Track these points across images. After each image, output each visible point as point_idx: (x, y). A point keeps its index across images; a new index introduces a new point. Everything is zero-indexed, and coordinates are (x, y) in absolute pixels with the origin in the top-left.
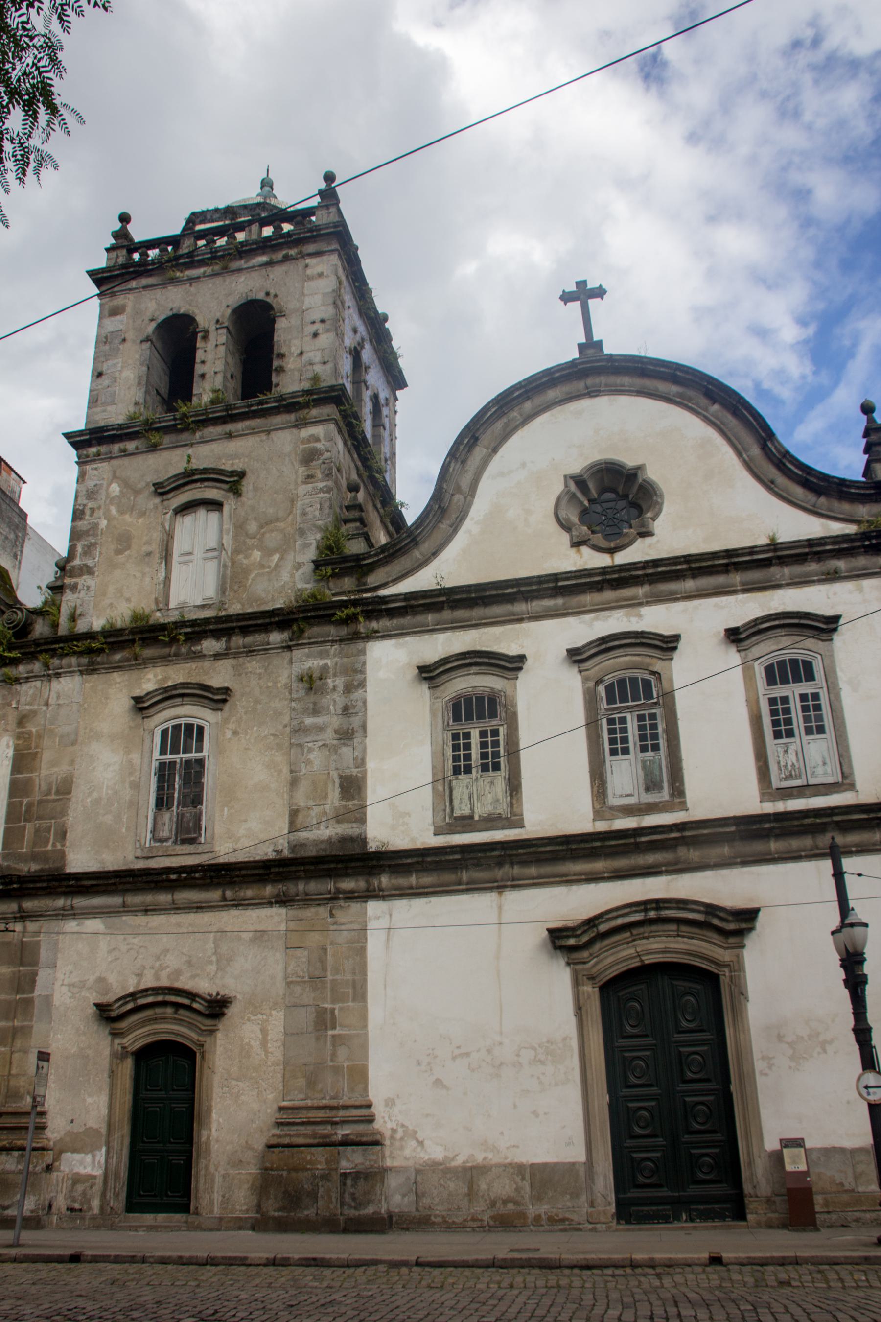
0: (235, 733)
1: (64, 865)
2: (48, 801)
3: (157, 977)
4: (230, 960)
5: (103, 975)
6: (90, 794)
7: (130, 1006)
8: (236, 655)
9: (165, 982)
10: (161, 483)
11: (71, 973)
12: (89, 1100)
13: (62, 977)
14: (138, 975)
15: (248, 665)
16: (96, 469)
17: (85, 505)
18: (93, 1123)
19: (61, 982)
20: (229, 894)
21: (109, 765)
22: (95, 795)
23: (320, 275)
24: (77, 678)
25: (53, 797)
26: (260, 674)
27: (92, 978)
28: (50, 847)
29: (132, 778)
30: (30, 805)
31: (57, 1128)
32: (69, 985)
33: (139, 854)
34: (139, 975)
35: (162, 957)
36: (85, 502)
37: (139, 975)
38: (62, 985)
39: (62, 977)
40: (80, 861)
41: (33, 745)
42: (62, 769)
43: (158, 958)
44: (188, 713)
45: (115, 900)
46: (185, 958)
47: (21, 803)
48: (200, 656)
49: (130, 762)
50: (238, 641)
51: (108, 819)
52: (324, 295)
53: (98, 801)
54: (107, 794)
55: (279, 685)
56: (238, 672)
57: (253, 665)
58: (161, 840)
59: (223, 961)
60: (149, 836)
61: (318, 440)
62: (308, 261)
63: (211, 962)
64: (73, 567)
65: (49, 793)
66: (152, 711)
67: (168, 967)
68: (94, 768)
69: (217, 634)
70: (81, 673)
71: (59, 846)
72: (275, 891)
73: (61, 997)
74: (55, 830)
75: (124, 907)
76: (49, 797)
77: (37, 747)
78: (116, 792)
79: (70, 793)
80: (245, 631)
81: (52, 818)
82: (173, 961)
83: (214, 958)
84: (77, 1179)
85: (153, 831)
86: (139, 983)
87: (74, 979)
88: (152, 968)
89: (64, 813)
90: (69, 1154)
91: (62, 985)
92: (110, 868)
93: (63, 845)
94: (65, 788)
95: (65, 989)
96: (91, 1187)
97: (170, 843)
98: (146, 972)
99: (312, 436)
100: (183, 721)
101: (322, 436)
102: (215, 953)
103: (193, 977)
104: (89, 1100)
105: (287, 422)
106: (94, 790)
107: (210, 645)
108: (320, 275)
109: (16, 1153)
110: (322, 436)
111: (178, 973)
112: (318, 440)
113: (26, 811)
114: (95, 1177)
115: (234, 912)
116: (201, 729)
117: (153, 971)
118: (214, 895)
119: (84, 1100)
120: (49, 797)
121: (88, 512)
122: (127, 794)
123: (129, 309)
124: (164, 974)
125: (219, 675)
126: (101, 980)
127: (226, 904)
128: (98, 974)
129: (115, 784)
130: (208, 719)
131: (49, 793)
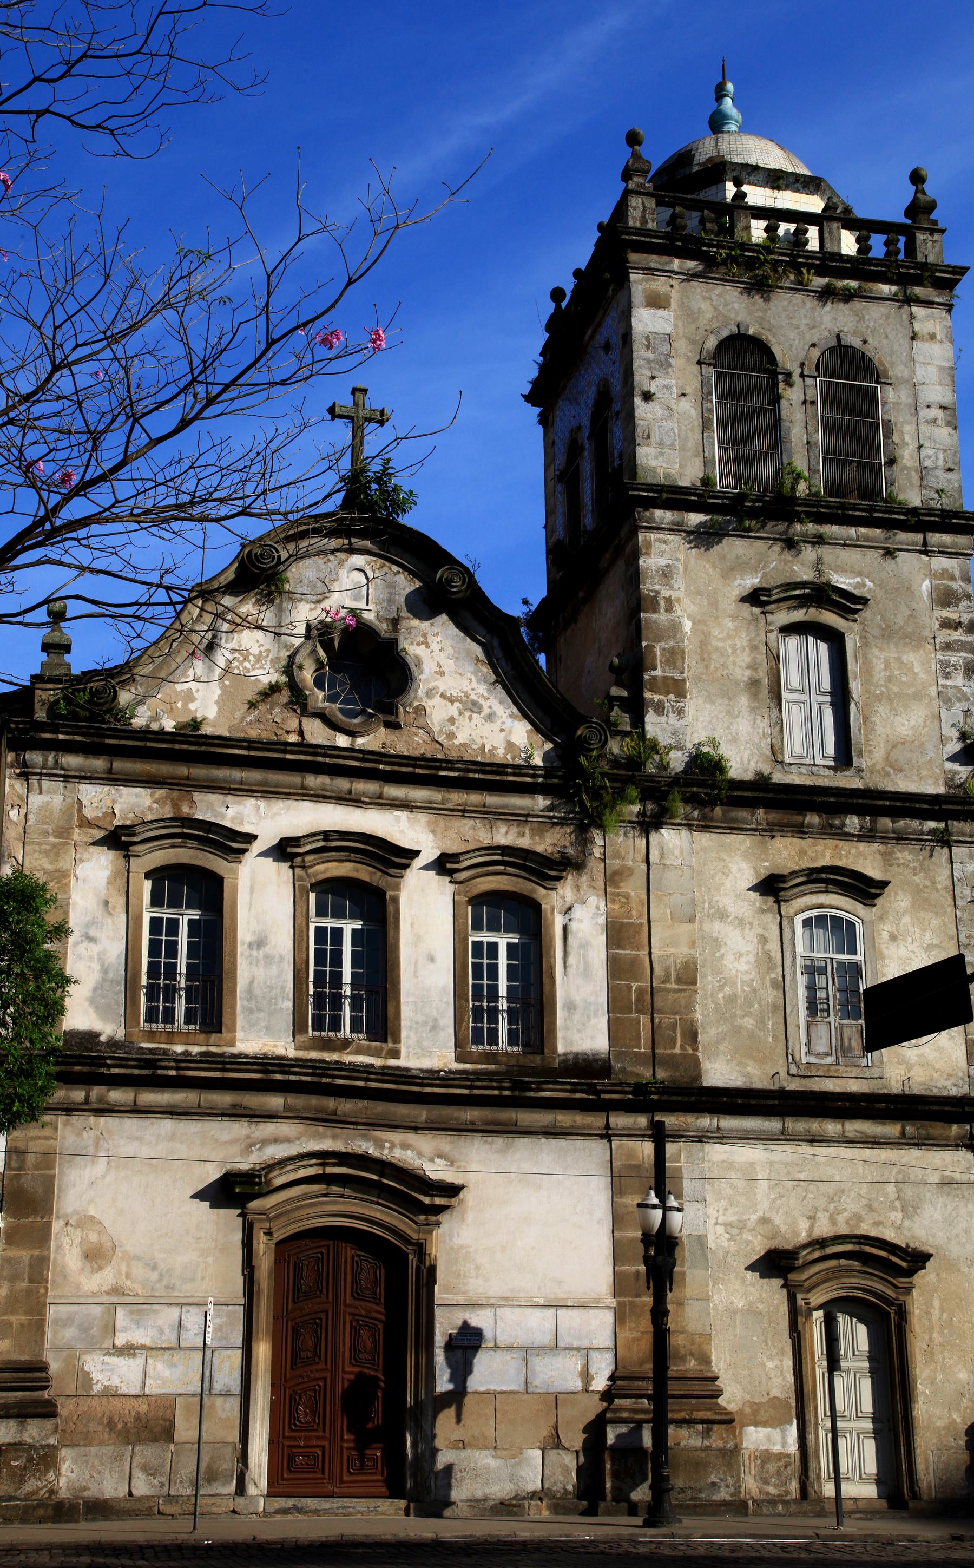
0: (893, 938)
1: (698, 1076)
2: (668, 991)
3: (834, 1222)
4: (915, 1208)
5: (767, 1215)
6: (721, 988)
7: (817, 1254)
8: (884, 839)
9: (844, 1230)
10: (769, 590)
11: (726, 1209)
12: (770, 1365)
13: (715, 1214)
14: (810, 1218)
15: (899, 855)
16: (665, 542)
17: (657, 592)
18: (775, 1392)
19: (714, 1221)
20: (909, 1130)
21: (741, 955)
22: (728, 990)
23: (933, 337)
24: (684, 833)
25: (674, 986)
26: (914, 869)
27: (754, 1218)
28: (677, 1050)
29: (773, 976)
30: (640, 992)
31: (732, 1397)
32: (725, 1225)
33: (793, 1070)
34: (812, 1218)
35: (836, 1199)
36: (657, 587)
37: (812, 1218)
38: (716, 1224)
39: (715, 1214)
40: (719, 1072)
41: (634, 912)
42: (682, 952)
43: (832, 1200)
44: (834, 903)
45: (774, 1125)
46: (864, 1202)
47: (630, 988)
48: (841, 834)
49: (768, 955)
50: (886, 823)
51: (749, 1023)
52: (941, 369)
53: (731, 999)
54: (743, 991)
55: (939, 887)
56: (887, 859)
57: (904, 854)
58: (818, 1055)
59: (909, 1209)
60: (804, 1049)
61: (953, 578)
62: (915, 309)
63: (894, 1209)
64: (654, 678)
65: (667, 979)
66: (789, 893)
67: (845, 1210)
68: (722, 956)
69: (860, 812)
70: (689, 827)
71: (691, 1052)
72: (962, 1132)
73: (717, 1238)
74: (682, 1029)
75: (782, 1133)
76: (668, 986)
77: (640, 916)
78: (755, 991)
79: (695, 983)
80: (895, 813)
81: (676, 1013)
82: (850, 1205)
83: (897, 1204)
84: (766, 1457)
85: (808, 1044)
86: (812, 1227)
87: (730, 1218)
88: (826, 1210)
89: (690, 1007)
90: (752, 1428)
91: (716, 1224)
92: (758, 1085)
93: (696, 1050)
94: (688, 976)
95: (720, 1229)
96: (786, 1467)
97: (830, 1060)
98: (819, 1215)
99: (945, 570)
100: (828, 912)
101: (957, 573)
102: (898, 1198)
103: (877, 1224)
104: (770, 1365)
105: (914, 544)
106: (725, 984)
107: (853, 823)
108: (933, 337)
109: (700, 1427)
110: (957, 573)
111: (858, 1218)
112: (953, 578)
113: (637, 1000)
114: (788, 1456)
115: (916, 1152)
116: (852, 926)
117: (827, 1215)
118: (892, 1129)
119: (763, 1365)
120: (668, 986)
121: (662, 603)
122: (772, 995)
123: (674, 303)
124: (841, 1219)
125: (865, 859)
126: (764, 1221)
127: (903, 1142)
128: (760, 1214)
129: (753, 981)
130: (861, 915)
131: (667, 979)
